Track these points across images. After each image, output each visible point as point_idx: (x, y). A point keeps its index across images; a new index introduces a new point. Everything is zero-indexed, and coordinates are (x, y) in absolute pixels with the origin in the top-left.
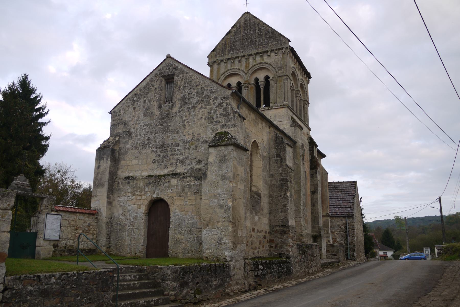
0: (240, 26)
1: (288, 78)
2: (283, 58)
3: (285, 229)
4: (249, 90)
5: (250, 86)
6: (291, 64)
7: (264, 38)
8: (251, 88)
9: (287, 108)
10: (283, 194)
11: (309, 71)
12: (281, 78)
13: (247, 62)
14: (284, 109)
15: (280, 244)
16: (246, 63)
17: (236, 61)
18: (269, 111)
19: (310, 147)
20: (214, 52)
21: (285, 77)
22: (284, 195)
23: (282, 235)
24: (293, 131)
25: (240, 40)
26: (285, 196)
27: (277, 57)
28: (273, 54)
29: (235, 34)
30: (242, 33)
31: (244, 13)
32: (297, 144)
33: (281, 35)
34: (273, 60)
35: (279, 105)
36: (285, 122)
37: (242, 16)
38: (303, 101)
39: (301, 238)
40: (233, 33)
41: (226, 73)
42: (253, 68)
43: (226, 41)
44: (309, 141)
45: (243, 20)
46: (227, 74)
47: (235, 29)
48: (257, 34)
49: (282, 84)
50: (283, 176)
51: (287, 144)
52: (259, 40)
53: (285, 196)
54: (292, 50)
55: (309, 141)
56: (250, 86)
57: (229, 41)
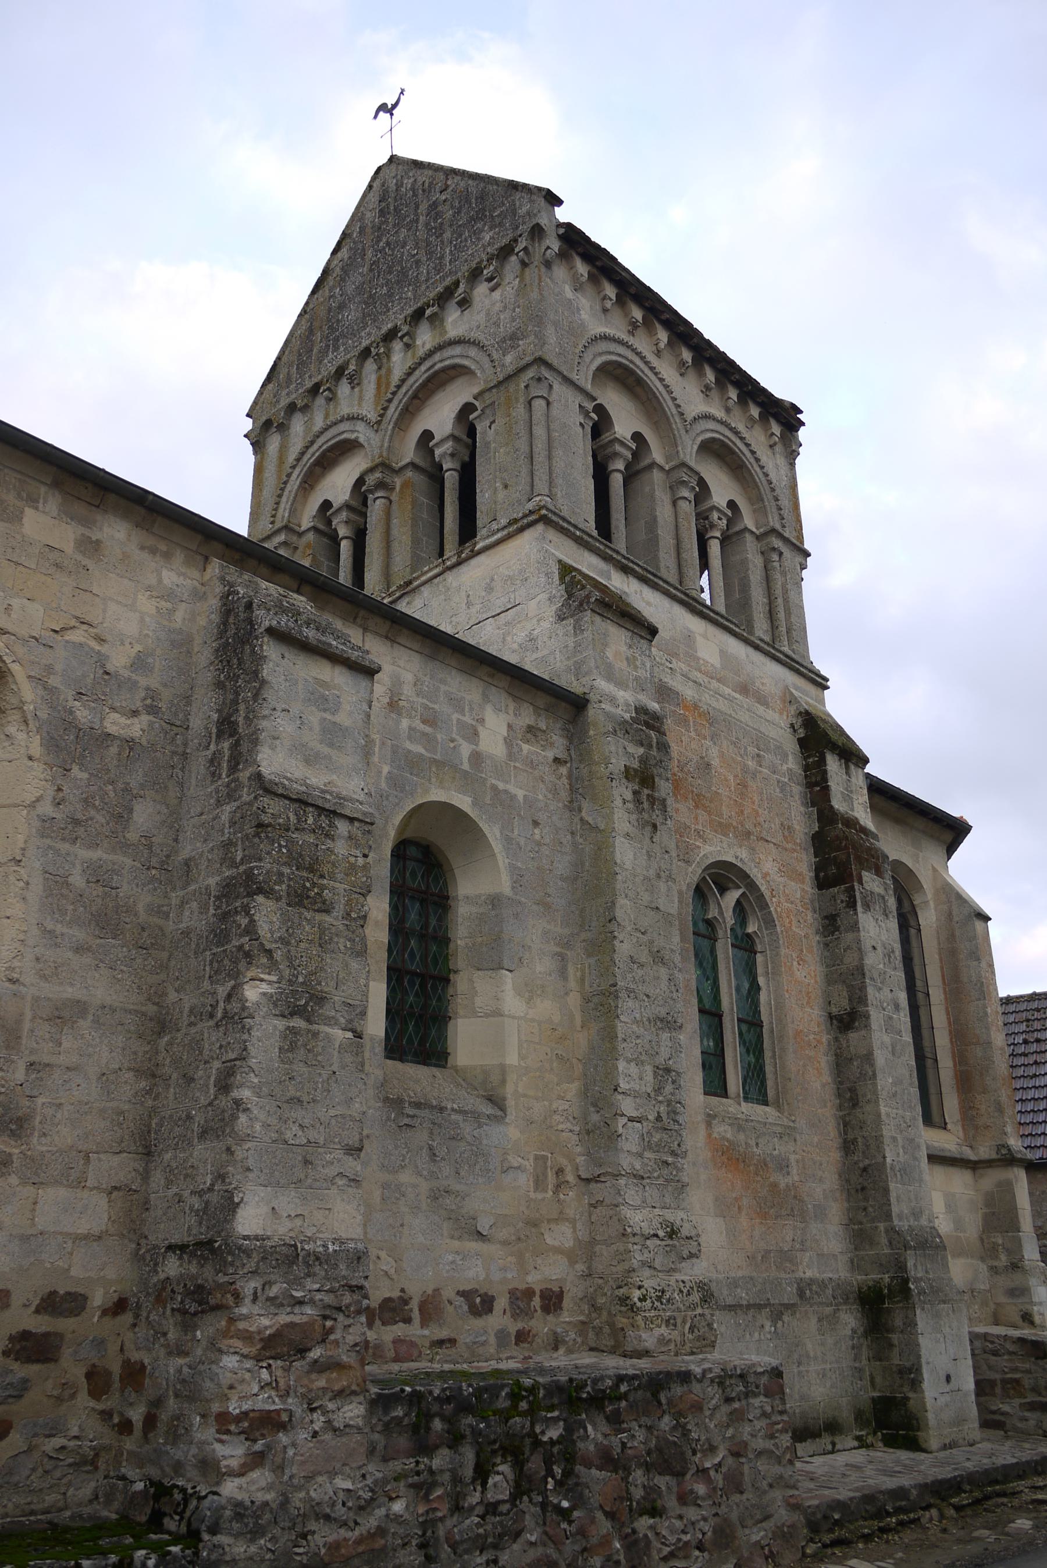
0: (362, 230)
1: (545, 373)
2: (522, 290)
3: (208, 1275)
4: (394, 497)
5: (398, 482)
6: (590, 314)
7: (447, 235)
8: (405, 485)
9: (540, 527)
10: (222, 991)
11: (780, 391)
12: (512, 388)
13: (383, 371)
14: (528, 535)
15: (172, 1403)
16: (379, 379)
17: (344, 389)
18: (464, 568)
19: (806, 768)
20: (270, 386)
21: (530, 373)
22: (229, 997)
23: (188, 1320)
24: (571, 642)
25: (360, 290)
26: (235, 1006)
27: (497, 295)
28: (481, 289)
29: (347, 269)
30: (369, 253)
31: (379, 169)
32: (591, 712)
33: (514, 186)
34: (483, 315)
35: (504, 522)
36: (533, 603)
37: (370, 186)
38: (758, 538)
39: (622, 1321)
40: (338, 270)
41: (305, 458)
42: (404, 389)
43: (311, 321)
44: (801, 732)
45: (374, 198)
46: (309, 458)
47: (344, 253)
48: (422, 234)
49: (520, 410)
50: (234, 865)
51: (271, 631)
52: (430, 254)
53: (235, 1006)
54: (574, 239)
55: (801, 732)
56: (398, 482)
57: (322, 312)
